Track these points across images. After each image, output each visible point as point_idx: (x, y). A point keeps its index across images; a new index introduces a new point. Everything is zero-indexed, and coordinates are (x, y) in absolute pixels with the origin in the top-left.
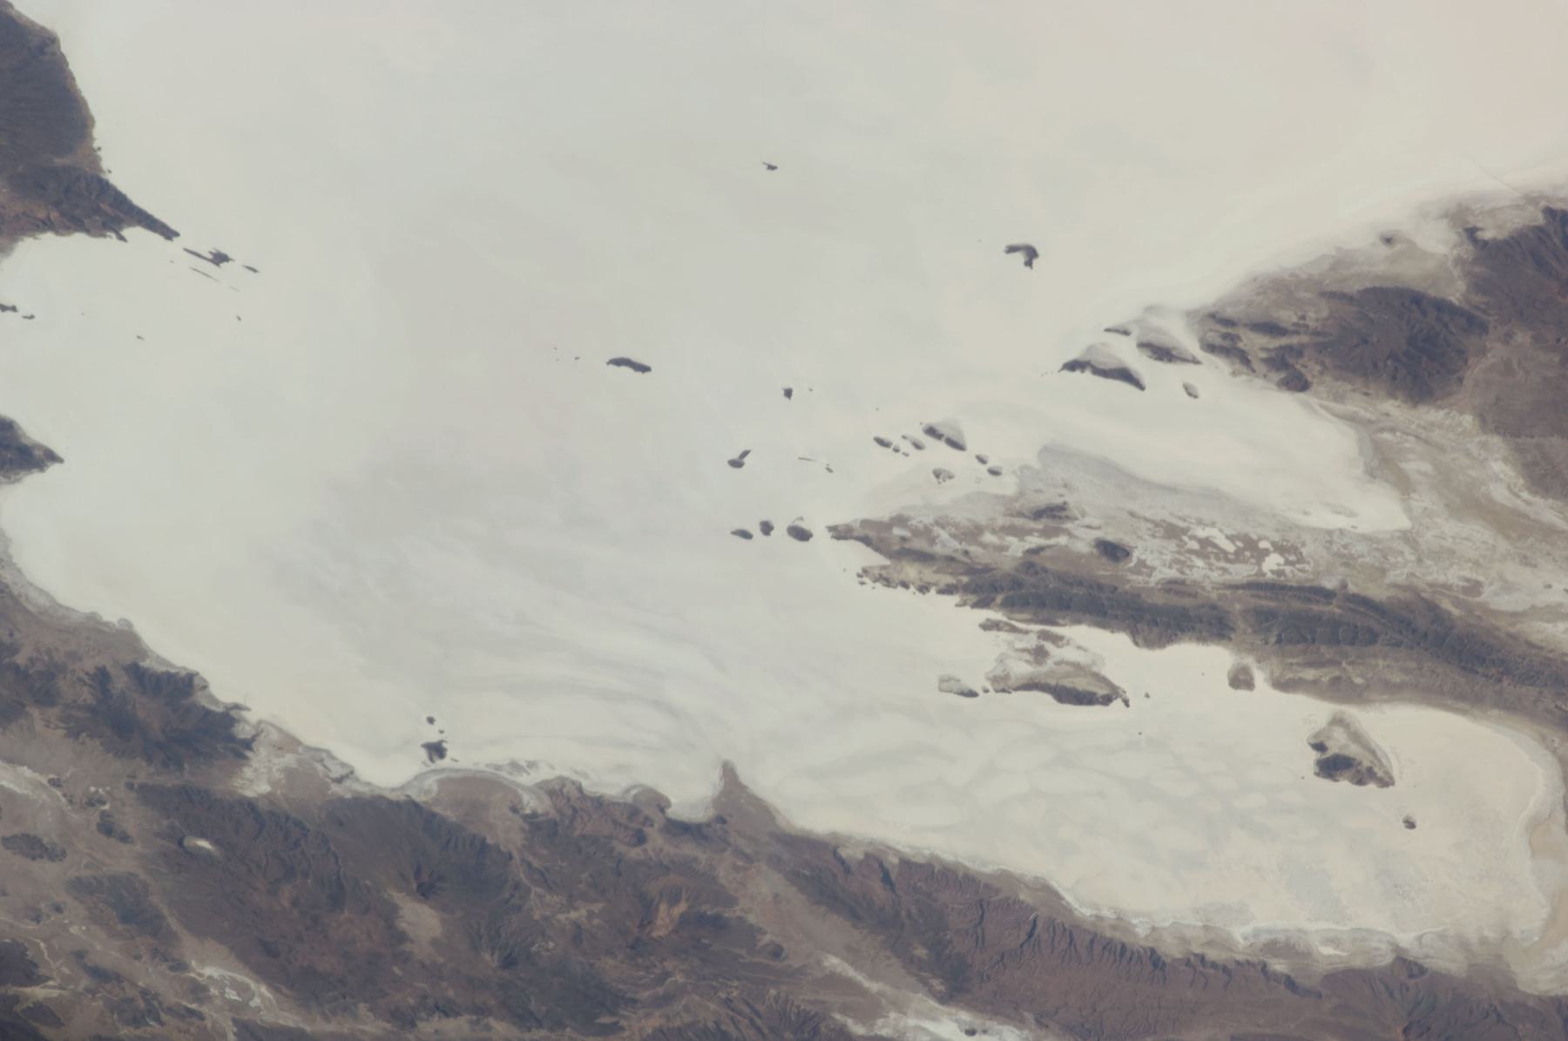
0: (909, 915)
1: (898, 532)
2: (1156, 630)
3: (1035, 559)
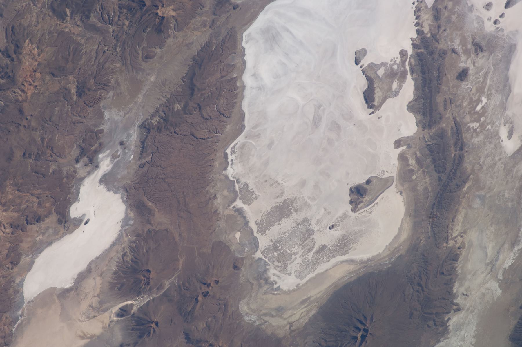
0: (202, 95)
2: (421, 106)
3: (449, 53)
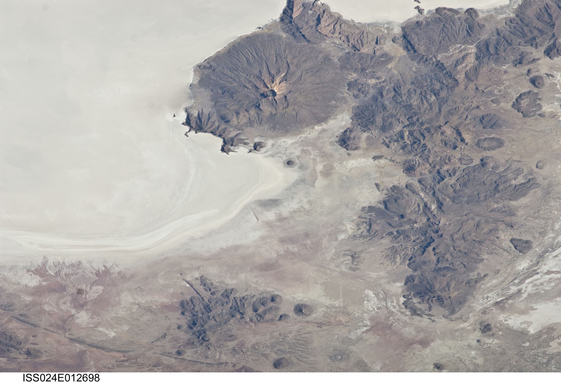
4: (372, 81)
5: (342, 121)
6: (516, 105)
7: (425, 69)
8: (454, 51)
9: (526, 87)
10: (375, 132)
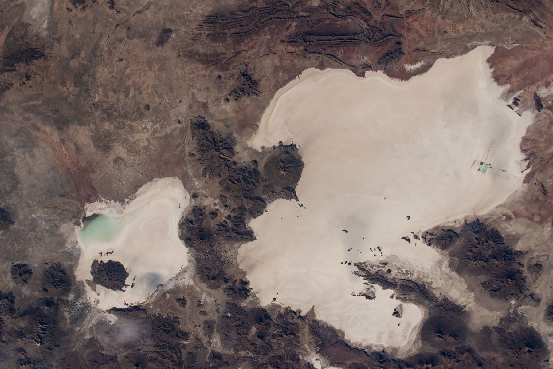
1: (363, 265)
4: (262, 184)
5: (261, 168)
6: (225, 197)
7: (253, 195)
8: (251, 205)
9: (227, 204)
10: (251, 170)
